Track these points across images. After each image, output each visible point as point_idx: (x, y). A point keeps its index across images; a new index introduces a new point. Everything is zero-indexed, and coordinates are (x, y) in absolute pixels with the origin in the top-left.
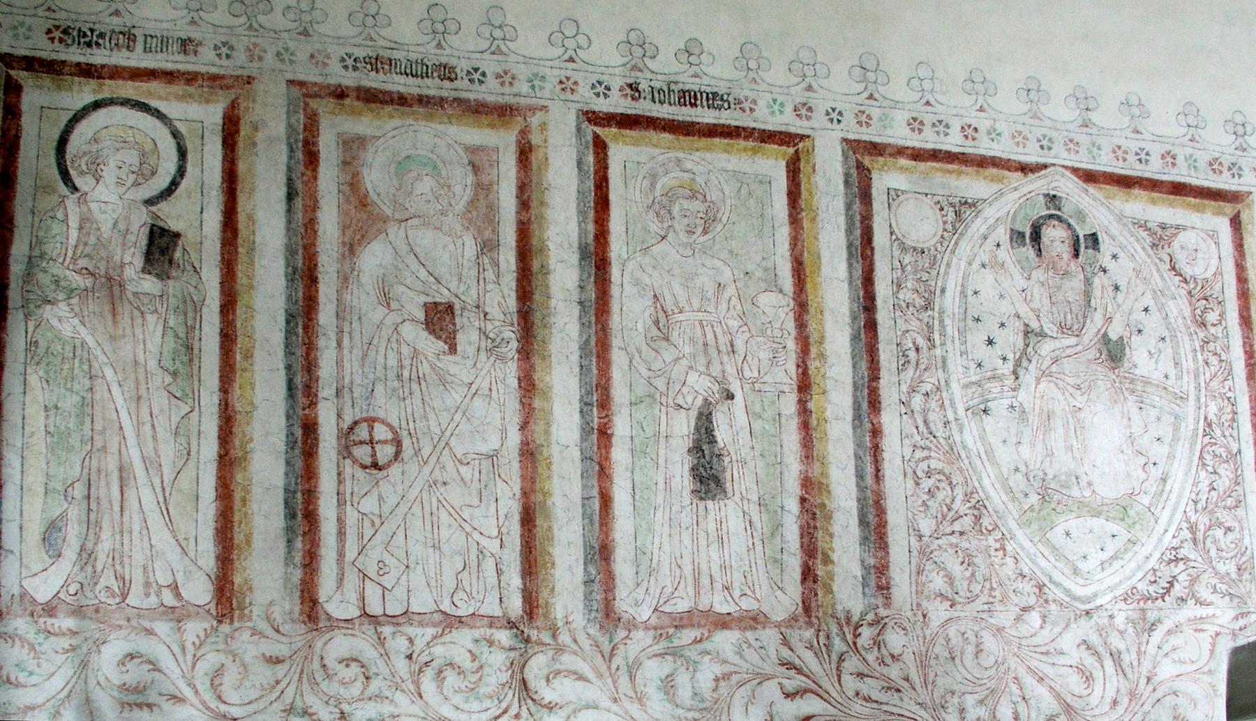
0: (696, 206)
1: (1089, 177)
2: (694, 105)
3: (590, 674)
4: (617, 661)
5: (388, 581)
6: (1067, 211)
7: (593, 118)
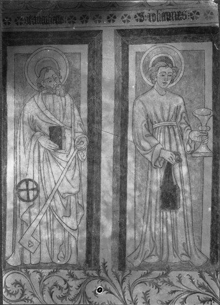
2: (168, 20)
3: (113, 290)
4: (125, 285)
5: (32, 249)
7: (122, 33)
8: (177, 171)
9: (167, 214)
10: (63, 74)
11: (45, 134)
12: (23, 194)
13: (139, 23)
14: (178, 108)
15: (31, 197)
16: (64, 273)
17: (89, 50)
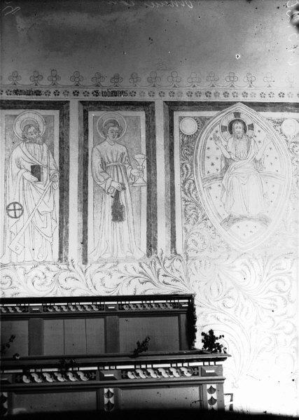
0: (116, 129)
1: (251, 105)
2: (116, 96)
3: (78, 277)
5: (17, 252)
6: (243, 117)
7: (83, 103)
8: (122, 194)
9: (118, 224)
10: (41, 130)
11: (27, 171)
12: (12, 213)
13: (95, 97)
14: (123, 154)
15: (17, 215)
16: (42, 268)
17: (60, 114)
